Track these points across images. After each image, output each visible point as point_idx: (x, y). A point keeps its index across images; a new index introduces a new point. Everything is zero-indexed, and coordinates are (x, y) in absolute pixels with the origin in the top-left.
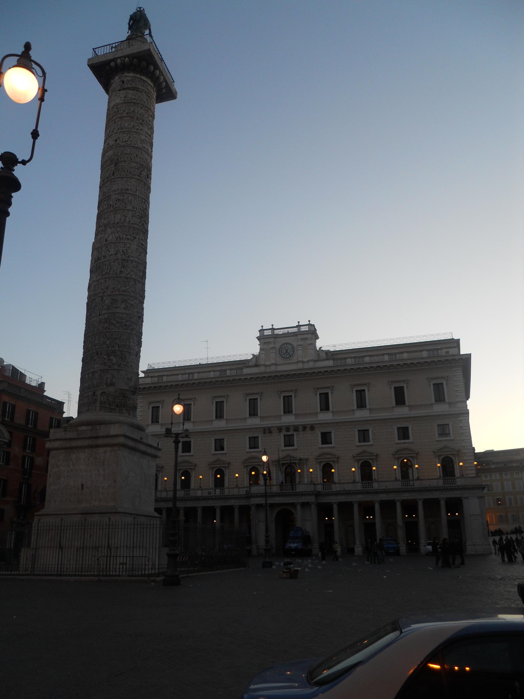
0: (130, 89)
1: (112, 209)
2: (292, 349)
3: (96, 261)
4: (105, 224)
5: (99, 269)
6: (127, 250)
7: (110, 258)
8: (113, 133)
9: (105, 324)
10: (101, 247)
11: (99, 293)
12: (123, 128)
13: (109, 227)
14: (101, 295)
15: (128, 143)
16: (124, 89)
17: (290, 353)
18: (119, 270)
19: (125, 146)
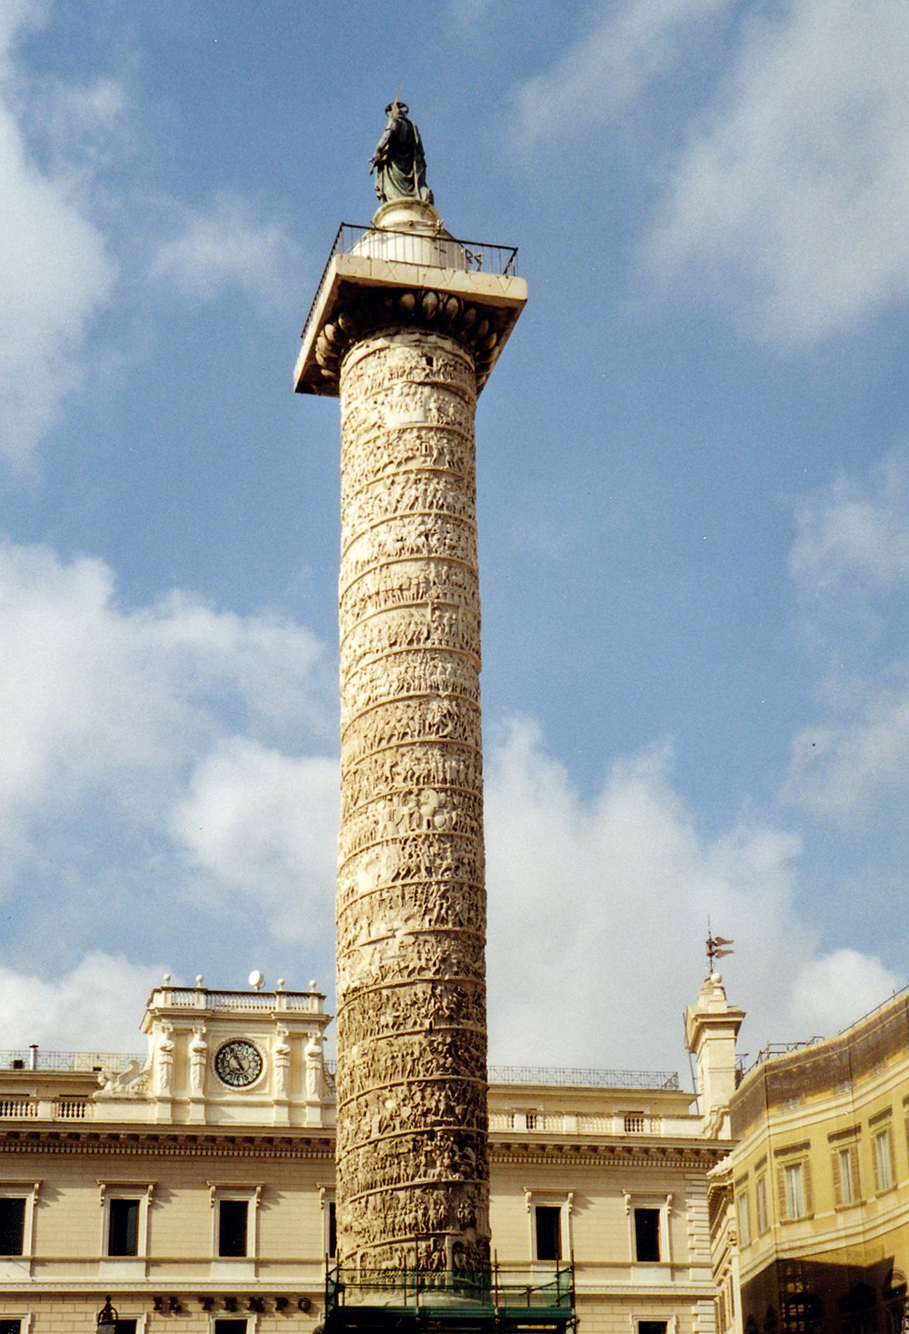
0: (449, 390)
1: (433, 737)
2: (256, 1061)
3: (398, 874)
4: (419, 777)
5: (416, 901)
6: (474, 861)
7: (446, 878)
8: (414, 511)
9: (447, 1059)
10: (414, 840)
11: (422, 969)
12: (443, 505)
13: (434, 789)
14: (429, 975)
15: (459, 553)
16: (434, 385)
17: (250, 1071)
18: (466, 916)
19: (453, 561)
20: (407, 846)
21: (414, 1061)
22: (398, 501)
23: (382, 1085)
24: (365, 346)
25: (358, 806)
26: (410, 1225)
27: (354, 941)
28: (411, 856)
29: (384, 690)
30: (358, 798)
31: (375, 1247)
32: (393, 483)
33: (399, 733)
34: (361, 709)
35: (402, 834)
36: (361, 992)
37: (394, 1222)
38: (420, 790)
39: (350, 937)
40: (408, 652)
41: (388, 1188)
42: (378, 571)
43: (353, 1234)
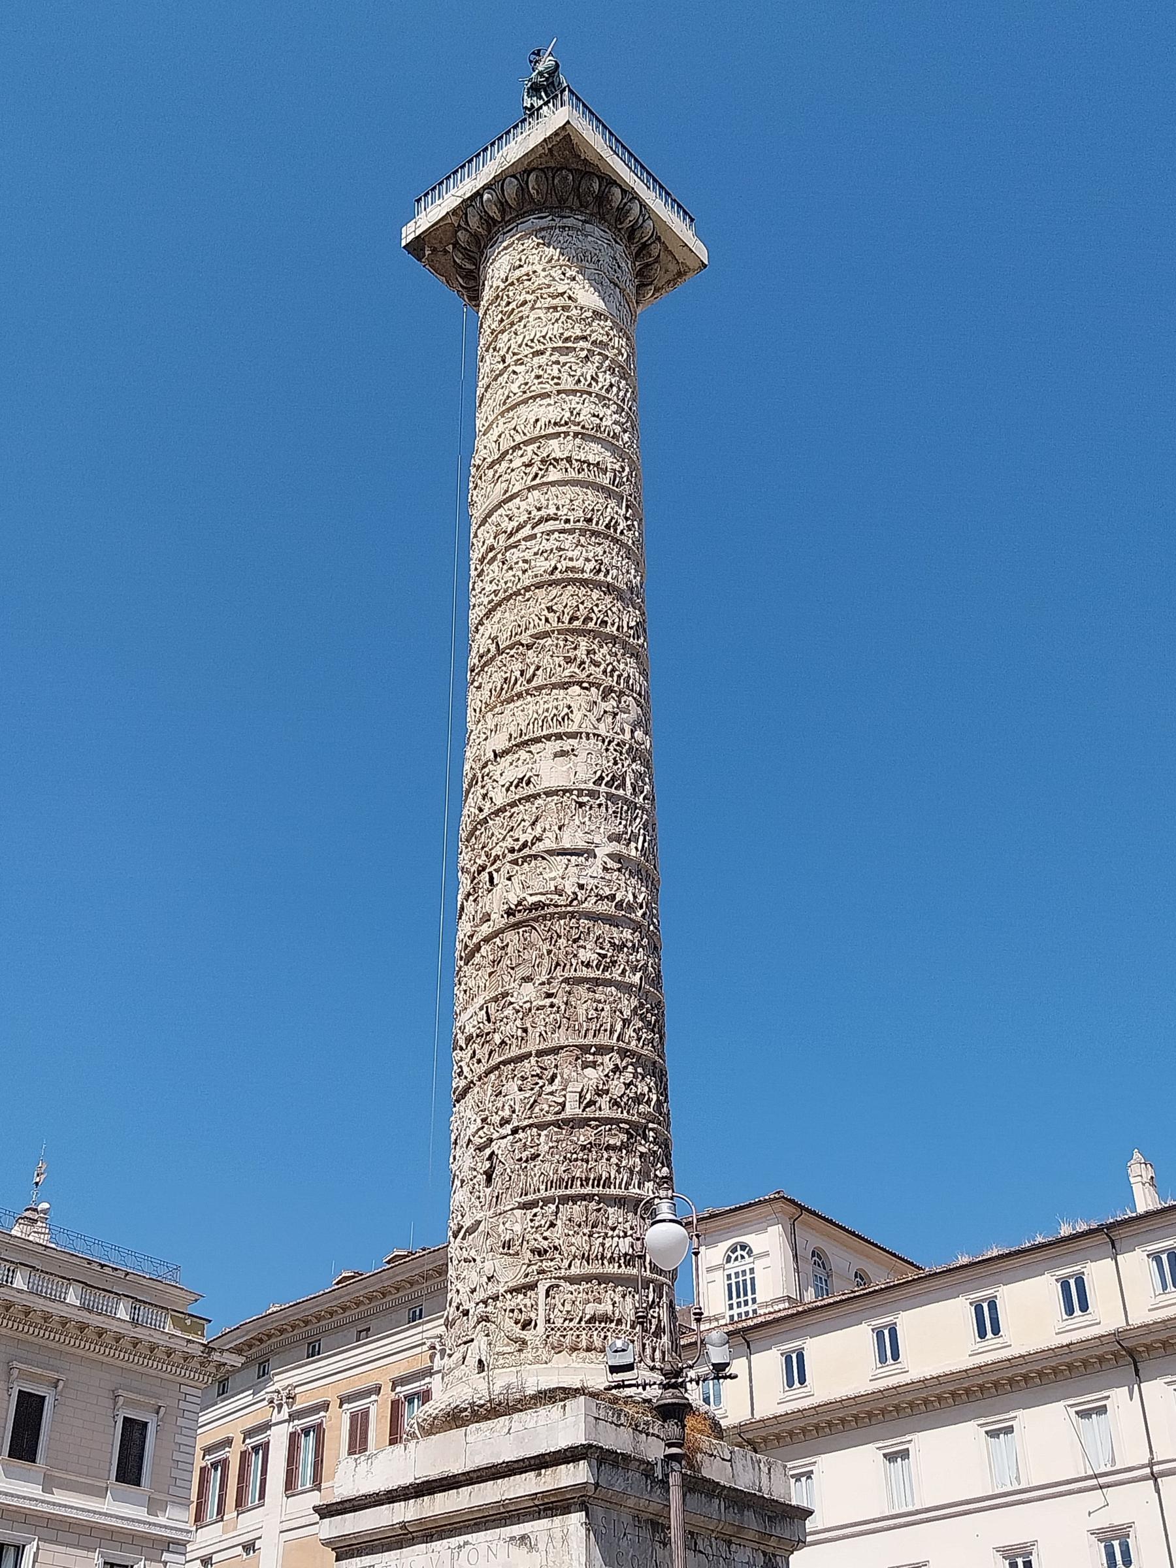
3: (601, 778)
10: (618, 745)
20: (611, 748)
21: (624, 1020)
22: (592, 378)
23: (581, 1041)
24: (550, 218)
25: (534, 684)
26: (626, 1254)
27: (533, 844)
28: (616, 763)
29: (579, 564)
30: (534, 675)
31: (572, 1280)
32: (587, 356)
33: (598, 619)
34: (541, 576)
35: (602, 730)
36: (547, 911)
37: (603, 1245)
38: (622, 693)
40: (607, 537)
41: (595, 1191)
42: (570, 438)
43: (529, 1254)
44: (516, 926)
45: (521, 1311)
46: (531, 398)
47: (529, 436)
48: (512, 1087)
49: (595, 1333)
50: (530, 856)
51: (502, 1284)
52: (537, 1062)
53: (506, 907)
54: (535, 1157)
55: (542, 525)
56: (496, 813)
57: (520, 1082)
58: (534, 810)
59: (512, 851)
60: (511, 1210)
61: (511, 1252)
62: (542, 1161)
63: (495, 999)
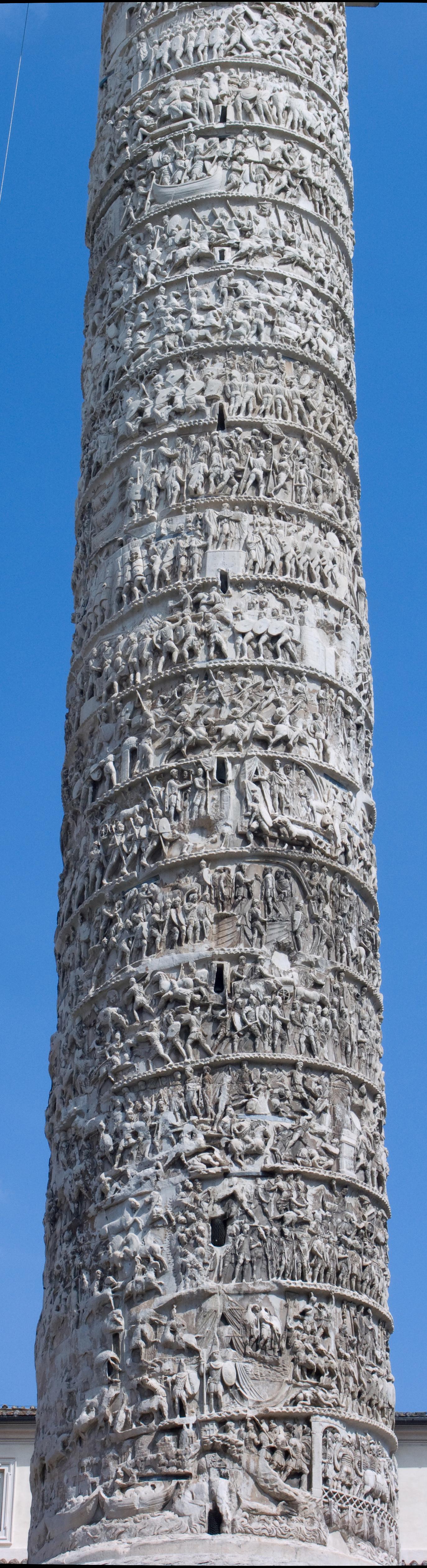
39: (283, 729)
44: (268, 859)
45: (287, 1455)
46: (274, 70)
47: (273, 126)
48: (260, 1103)
49: (375, 1515)
50: (292, 762)
51: (251, 1404)
52: (304, 1079)
53: (255, 825)
54: (302, 1223)
55: (289, 266)
56: (230, 670)
57: (276, 1101)
58: (290, 693)
59: (263, 742)
60: (267, 1293)
61: (267, 1358)
62: (312, 1234)
63: (235, 959)
